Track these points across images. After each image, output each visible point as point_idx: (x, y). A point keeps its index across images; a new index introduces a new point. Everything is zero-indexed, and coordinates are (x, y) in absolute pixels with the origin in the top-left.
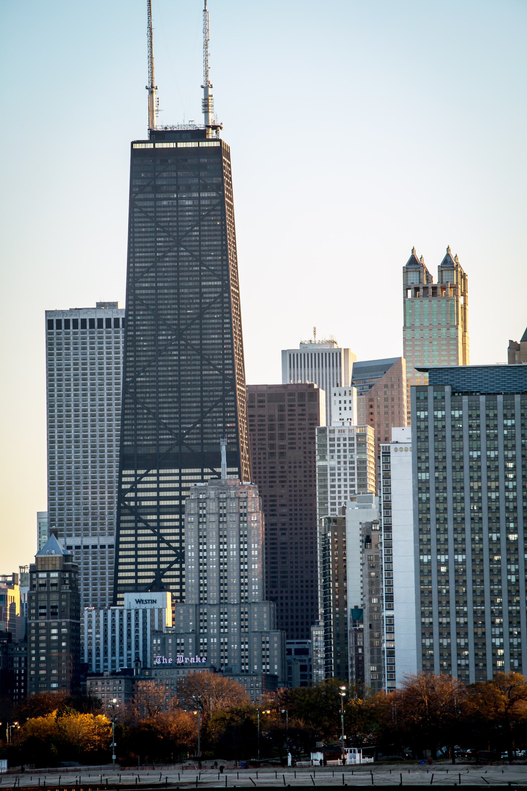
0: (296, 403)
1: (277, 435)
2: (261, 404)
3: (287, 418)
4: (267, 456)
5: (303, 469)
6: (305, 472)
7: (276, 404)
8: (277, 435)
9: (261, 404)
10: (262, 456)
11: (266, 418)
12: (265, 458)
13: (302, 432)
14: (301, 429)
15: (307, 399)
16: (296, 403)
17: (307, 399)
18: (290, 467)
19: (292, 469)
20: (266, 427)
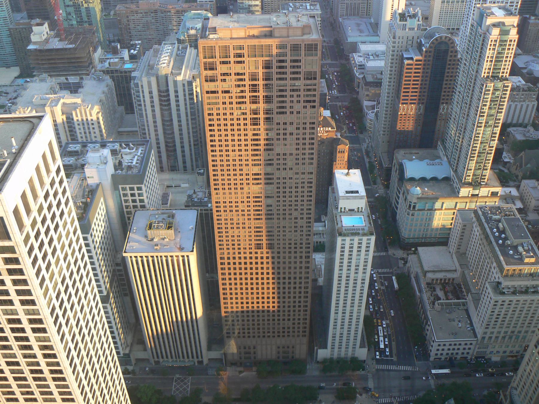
0: (288, 58)
1: (261, 98)
2: (239, 59)
3: (275, 76)
4: (248, 122)
5: (295, 136)
6: (298, 139)
7: (260, 60)
8: (261, 98)
9: (239, 59)
10: (242, 122)
11: (246, 77)
12: (245, 124)
13: (295, 94)
14: (293, 90)
15: (303, 52)
16: (288, 58)
17: (303, 52)
18: (278, 134)
19: (281, 137)
20: (247, 88)
